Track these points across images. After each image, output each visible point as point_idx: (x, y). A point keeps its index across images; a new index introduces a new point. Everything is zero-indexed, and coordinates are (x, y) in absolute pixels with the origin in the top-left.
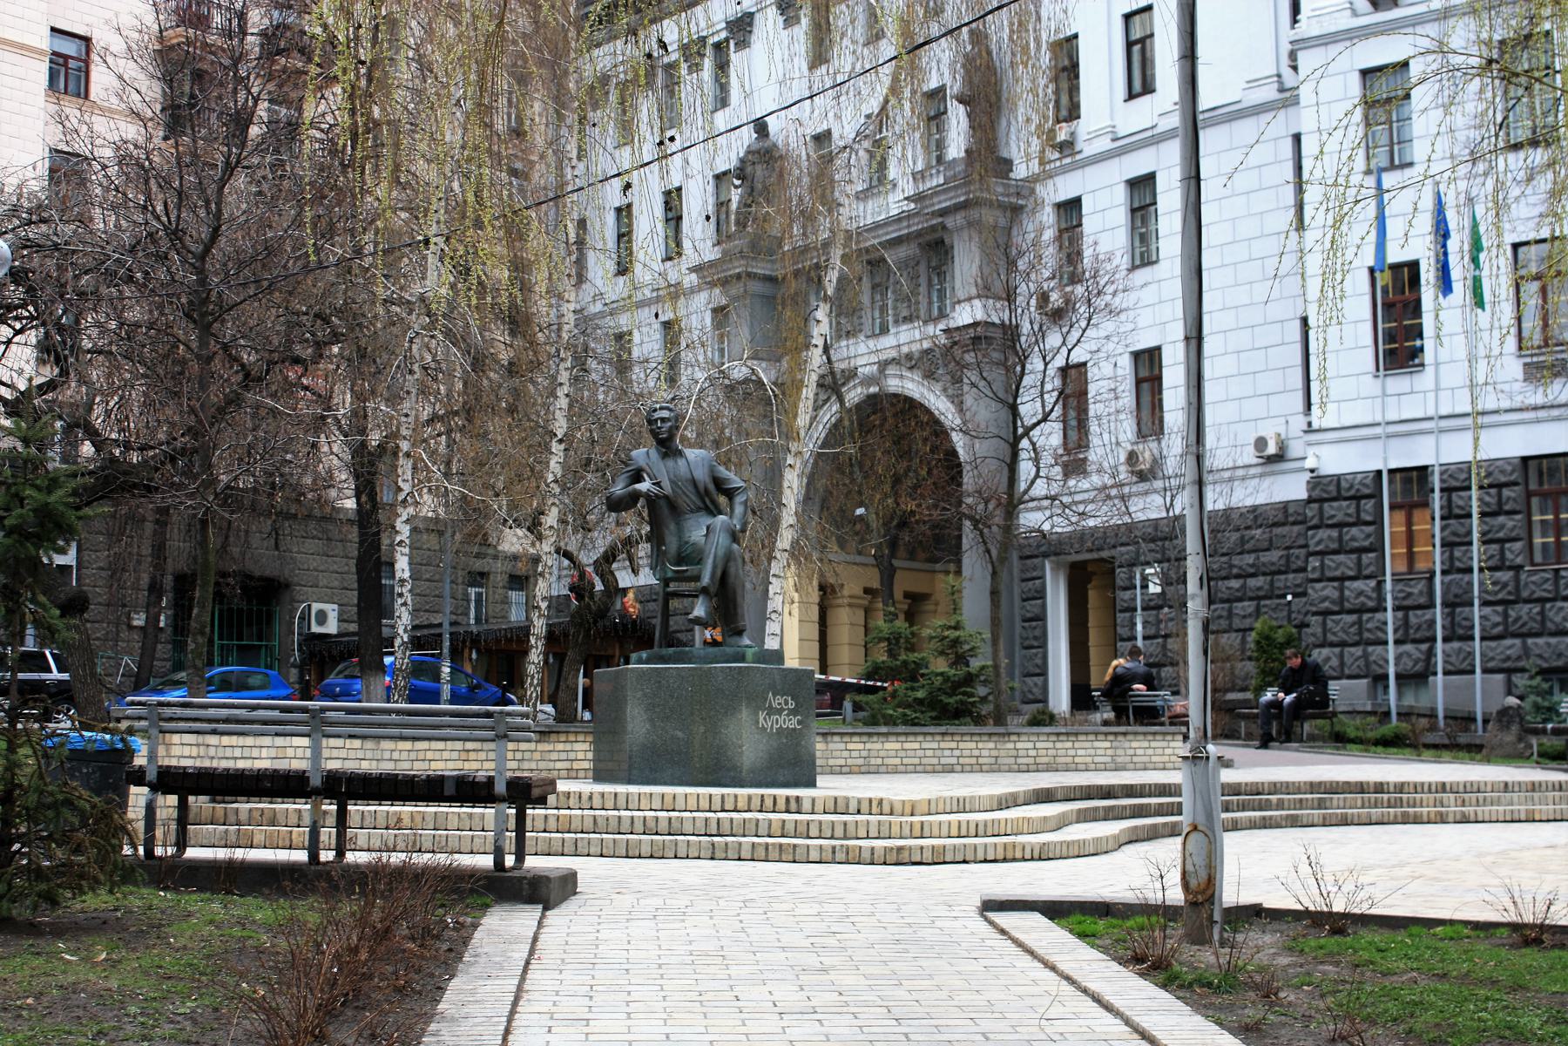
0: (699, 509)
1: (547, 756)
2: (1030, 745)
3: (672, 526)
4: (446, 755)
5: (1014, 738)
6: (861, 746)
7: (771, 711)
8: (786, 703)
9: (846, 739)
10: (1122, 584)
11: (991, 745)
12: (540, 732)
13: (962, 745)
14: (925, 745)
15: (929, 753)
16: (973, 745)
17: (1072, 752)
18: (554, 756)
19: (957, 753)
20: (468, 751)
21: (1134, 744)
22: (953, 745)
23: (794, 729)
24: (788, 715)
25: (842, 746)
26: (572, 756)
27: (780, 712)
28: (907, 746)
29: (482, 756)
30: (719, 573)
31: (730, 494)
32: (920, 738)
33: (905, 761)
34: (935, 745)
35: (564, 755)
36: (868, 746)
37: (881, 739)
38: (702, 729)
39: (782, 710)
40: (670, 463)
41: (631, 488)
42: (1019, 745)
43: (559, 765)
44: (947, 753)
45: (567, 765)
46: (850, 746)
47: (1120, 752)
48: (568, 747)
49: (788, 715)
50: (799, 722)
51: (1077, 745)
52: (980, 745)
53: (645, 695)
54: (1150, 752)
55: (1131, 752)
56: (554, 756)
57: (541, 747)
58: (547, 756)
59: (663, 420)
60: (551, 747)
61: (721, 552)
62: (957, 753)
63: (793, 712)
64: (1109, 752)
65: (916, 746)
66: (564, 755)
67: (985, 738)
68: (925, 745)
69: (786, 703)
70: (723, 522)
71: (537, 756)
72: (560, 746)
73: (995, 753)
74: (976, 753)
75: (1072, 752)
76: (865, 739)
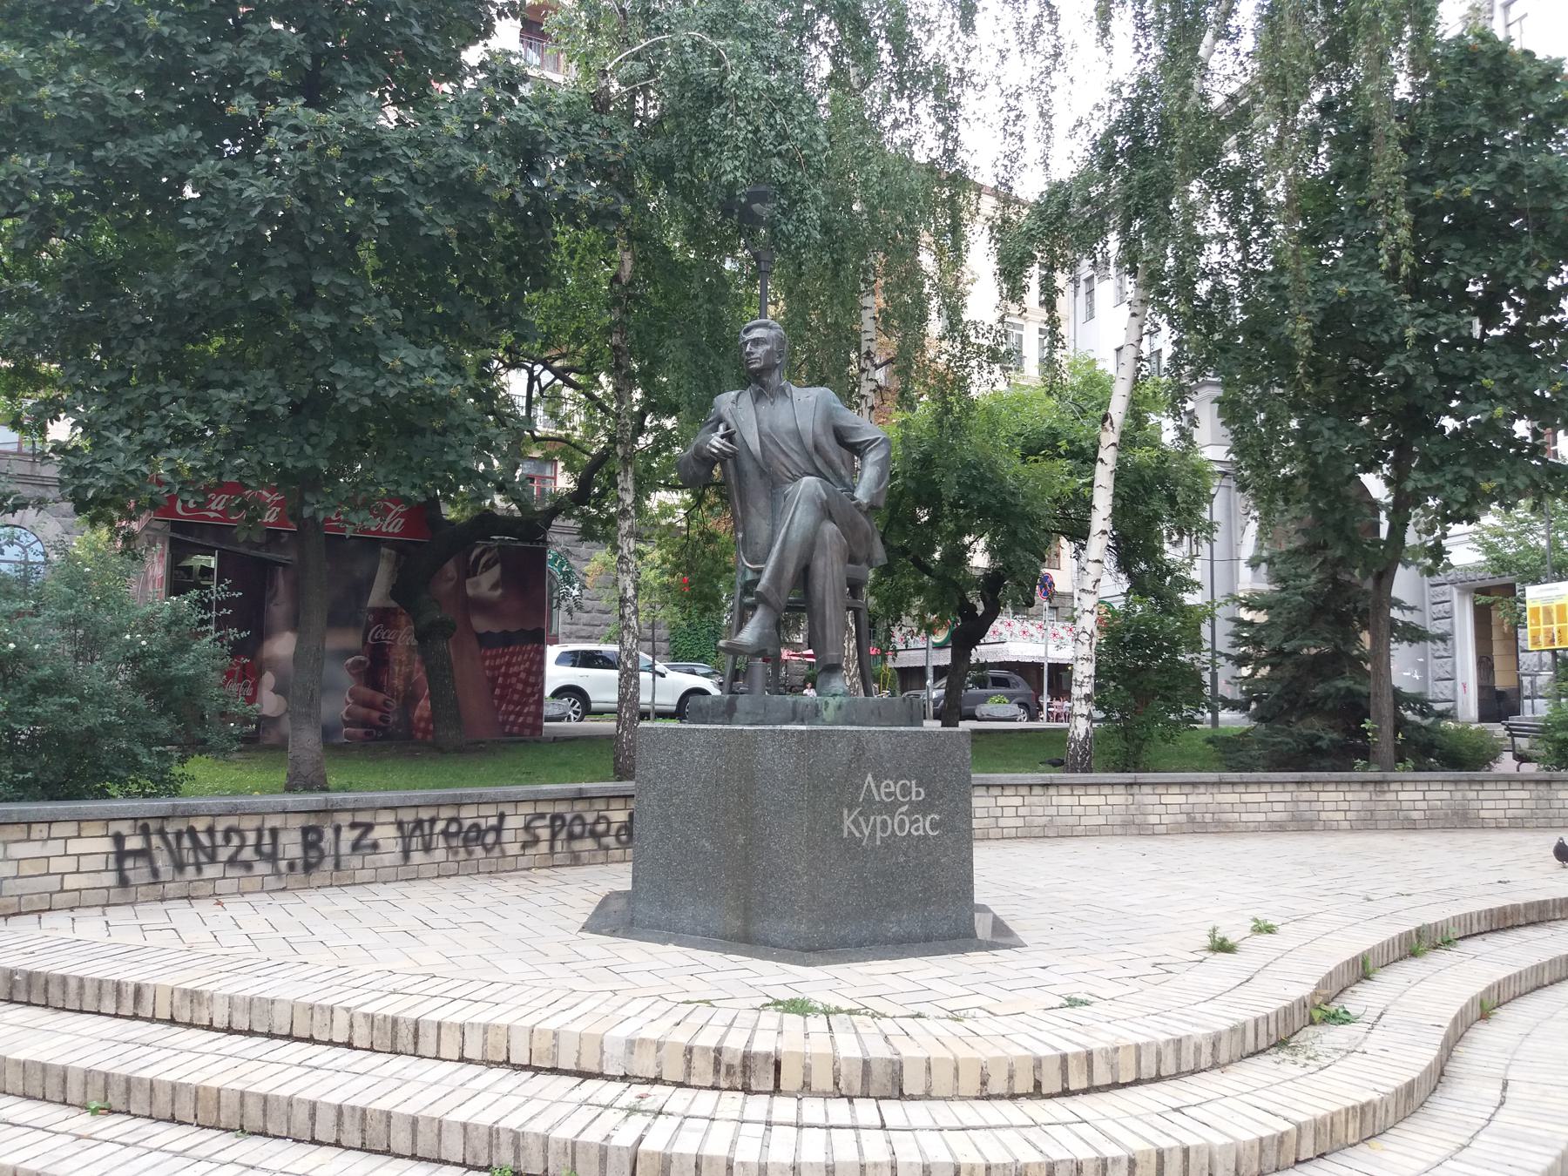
2: (1419, 796)
3: (762, 503)
5: (1394, 787)
6: (1182, 799)
7: (870, 806)
8: (906, 791)
9: (1160, 790)
13: (1323, 796)
14: (1272, 797)
22: (1313, 796)
24: (909, 813)
25: (1155, 799)
27: (891, 808)
28: (1246, 798)
30: (791, 569)
31: (858, 450)
32: (1266, 788)
36: (1192, 799)
37: (1210, 789)
38: (741, 839)
39: (895, 805)
40: (764, 408)
42: (1402, 796)
46: (1165, 799)
49: (909, 813)
50: (934, 826)
51: (1482, 795)
59: (756, 342)
61: (796, 536)
65: (1260, 798)
68: (1272, 797)
69: (906, 791)
70: (807, 485)
73: (1371, 806)
74: (1344, 806)
76: (1187, 789)
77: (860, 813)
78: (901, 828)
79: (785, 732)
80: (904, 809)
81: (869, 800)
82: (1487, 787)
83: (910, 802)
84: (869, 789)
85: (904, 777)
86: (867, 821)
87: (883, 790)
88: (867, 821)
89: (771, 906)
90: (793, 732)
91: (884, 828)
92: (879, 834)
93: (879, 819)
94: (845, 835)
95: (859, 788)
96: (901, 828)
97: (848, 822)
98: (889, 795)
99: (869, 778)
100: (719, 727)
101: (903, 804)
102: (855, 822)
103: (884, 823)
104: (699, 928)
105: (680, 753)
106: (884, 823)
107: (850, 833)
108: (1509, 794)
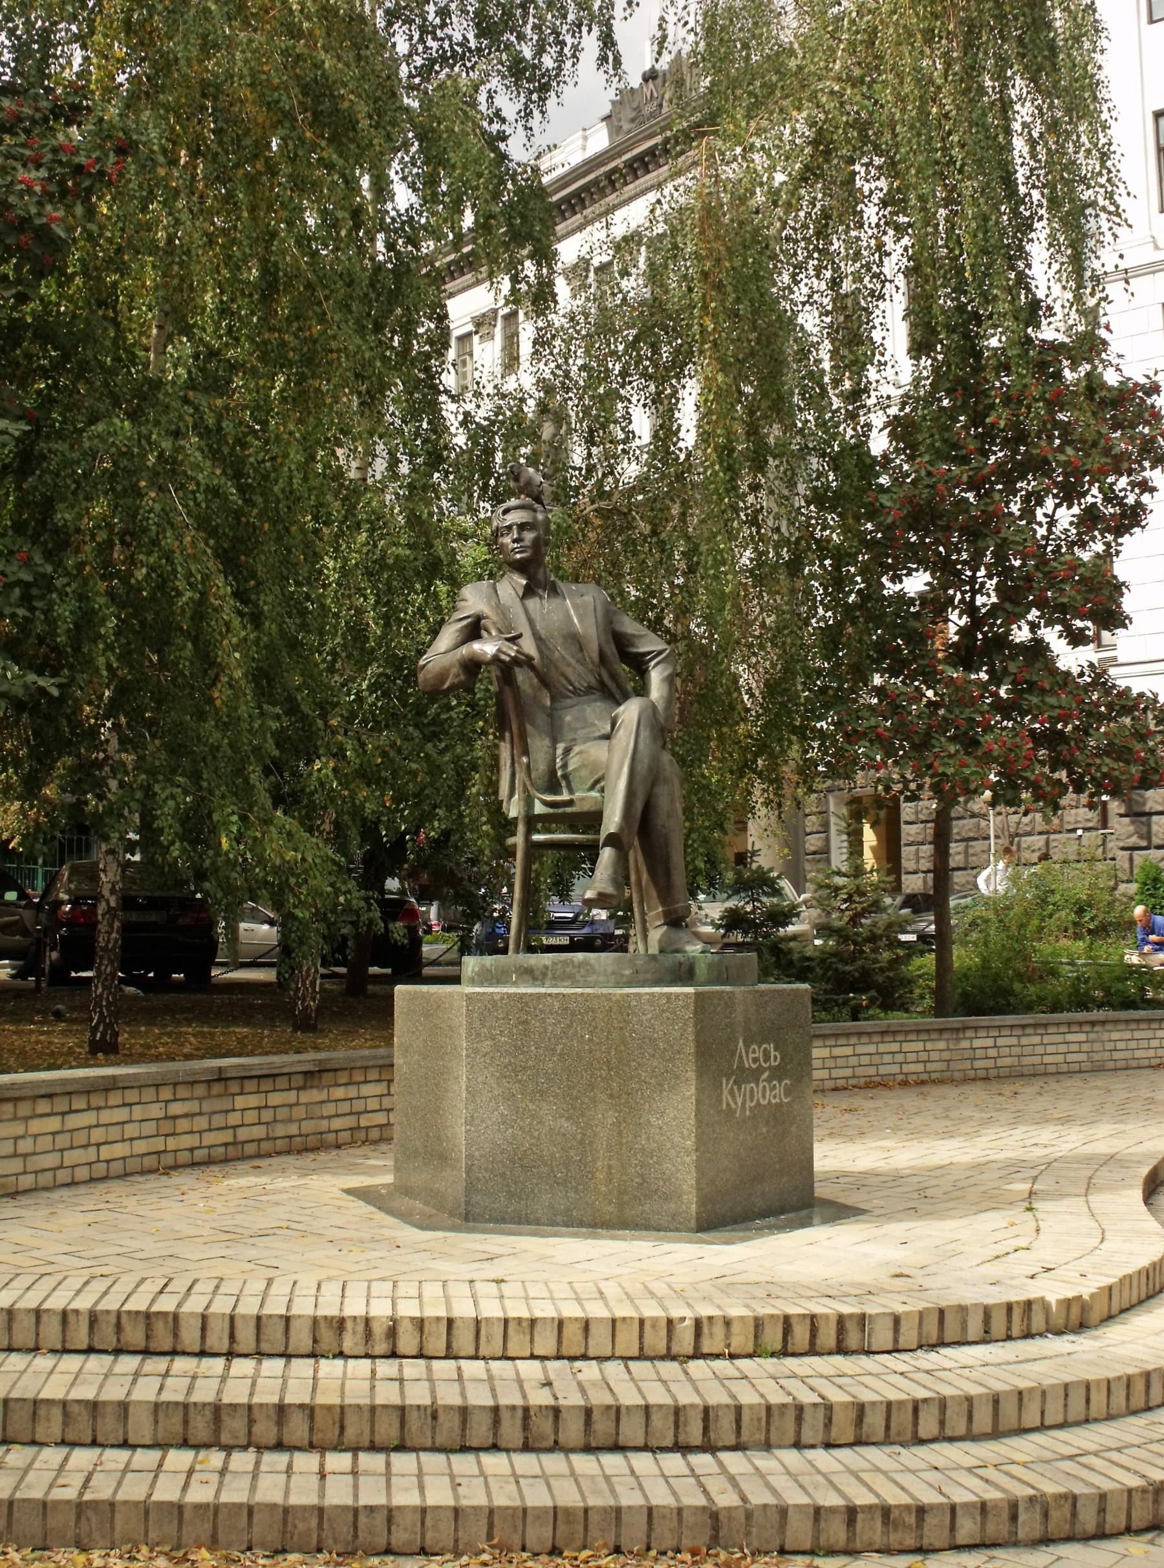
0: (590, 690)
1: (317, 1111)
2: (989, 1042)
4: (131, 1130)
5: (970, 1033)
8: (767, 1057)
10: (908, 819)
11: (942, 1045)
12: (305, 1073)
13: (907, 1047)
15: (865, 1060)
16: (919, 1046)
17: (1039, 1050)
18: (329, 1109)
19: (899, 1058)
20: (175, 1117)
21: (1115, 1036)
22: (895, 1047)
23: (780, 1105)
24: (769, 1080)
26: (359, 1105)
27: (755, 1075)
28: (837, 1051)
29: (202, 1123)
30: (639, 805)
33: (835, 1073)
34: (871, 1049)
35: (344, 1107)
39: (760, 1070)
41: (464, 650)
42: (977, 1043)
43: (337, 1124)
44: (887, 1058)
45: (350, 1121)
47: (1097, 1047)
48: (352, 1092)
49: (769, 1080)
51: (1046, 1039)
52: (929, 1046)
53: (497, 1048)
54: (1133, 1044)
55: (1110, 1046)
56: (329, 1109)
57: (305, 1097)
58: (317, 1111)
60: (323, 1096)
62: (899, 1058)
63: (778, 1073)
64: (1085, 1047)
65: (848, 1051)
66: (344, 1107)
67: (934, 1036)
68: (860, 1049)
69: (767, 1057)
71: (300, 1112)
72: (339, 1093)
74: (924, 1056)
75: (1039, 1050)
77: (735, 1082)
78: (764, 1096)
79: (668, 996)
80: (765, 1075)
81: (741, 1067)
82: (1051, 1030)
83: (770, 1068)
84: (741, 1057)
85: (766, 1040)
86: (739, 1089)
87: (751, 1056)
88: (739, 1089)
89: (654, 1187)
90: (677, 996)
91: (752, 1100)
92: (748, 1104)
93: (749, 1087)
94: (724, 1106)
95: (733, 1054)
96: (764, 1096)
97: (726, 1095)
98: (755, 1060)
99: (741, 1044)
100: (579, 990)
101: (765, 1069)
102: (731, 1092)
103: (752, 1089)
104: (559, 1218)
105: (526, 1022)
106: (752, 1089)
107: (728, 1104)
108: (1070, 1037)
